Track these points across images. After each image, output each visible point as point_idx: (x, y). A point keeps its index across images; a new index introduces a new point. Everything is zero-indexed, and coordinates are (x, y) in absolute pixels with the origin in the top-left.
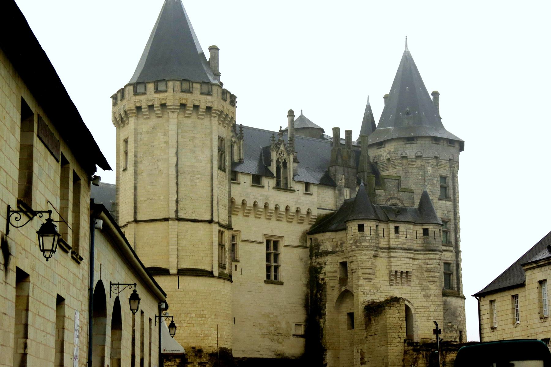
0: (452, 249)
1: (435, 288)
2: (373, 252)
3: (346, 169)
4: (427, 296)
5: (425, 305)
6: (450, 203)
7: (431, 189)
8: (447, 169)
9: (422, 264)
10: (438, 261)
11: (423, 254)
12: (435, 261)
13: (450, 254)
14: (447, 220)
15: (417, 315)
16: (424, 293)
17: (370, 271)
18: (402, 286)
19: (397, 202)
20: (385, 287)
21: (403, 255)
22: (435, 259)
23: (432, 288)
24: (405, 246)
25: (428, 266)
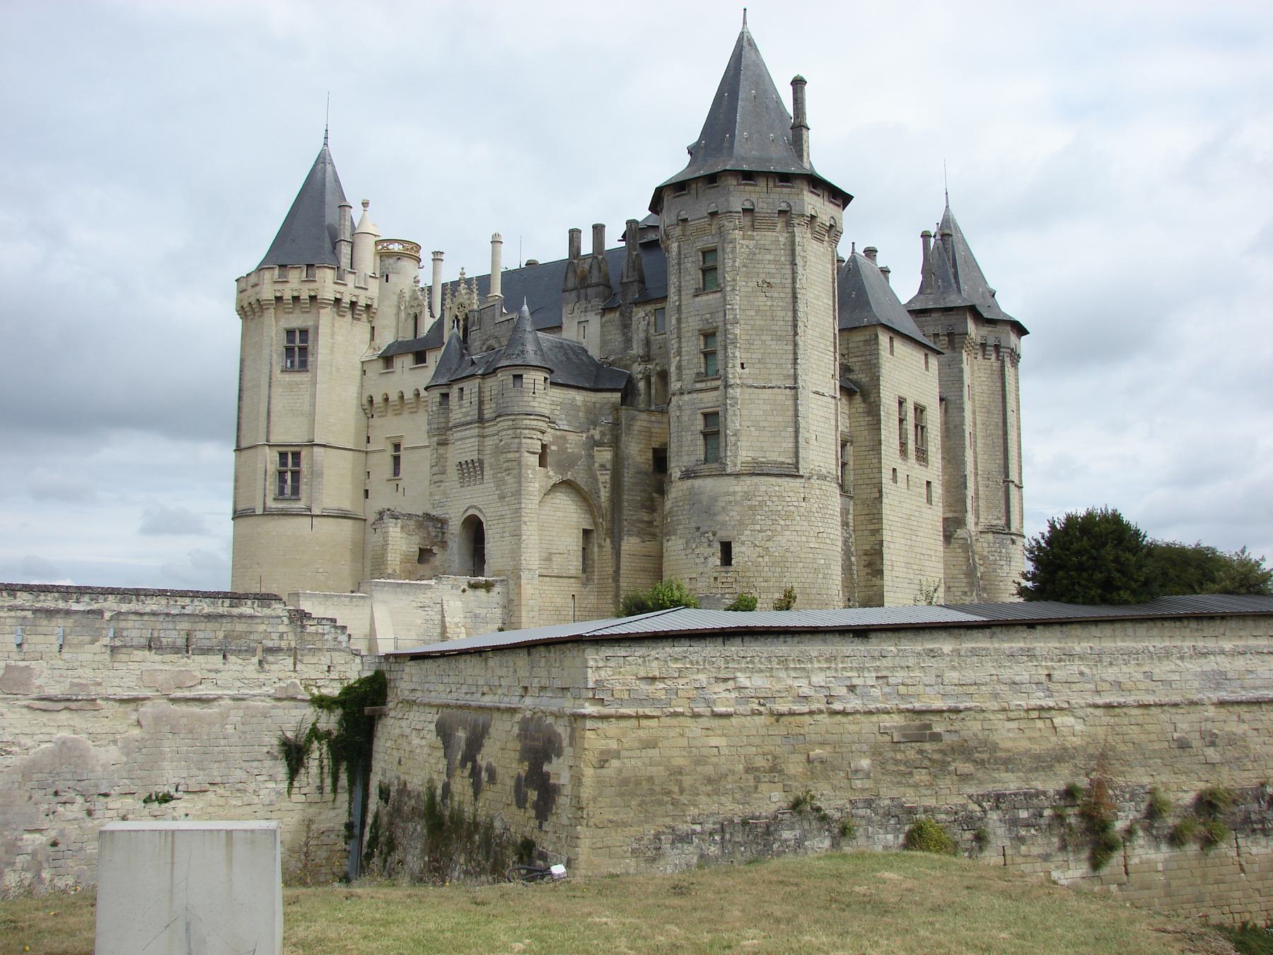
0: (718, 383)
1: (512, 481)
2: (435, 439)
3: (582, 292)
4: (502, 497)
5: (499, 514)
6: (719, 295)
7: (674, 283)
8: (714, 232)
9: (498, 441)
10: (510, 432)
11: (496, 425)
12: (504, 433)
13: (715, 393)
14: (711, 331)
15: (490, 532)
16: (498, 492)
17: (436, 468)
18: (475, 485)
19: (492, 342)
20: (454, 491)
21: (467, 432)
22: (504, 430)
23: (509, 482)
24: (468, 418)
25: (502, 443)
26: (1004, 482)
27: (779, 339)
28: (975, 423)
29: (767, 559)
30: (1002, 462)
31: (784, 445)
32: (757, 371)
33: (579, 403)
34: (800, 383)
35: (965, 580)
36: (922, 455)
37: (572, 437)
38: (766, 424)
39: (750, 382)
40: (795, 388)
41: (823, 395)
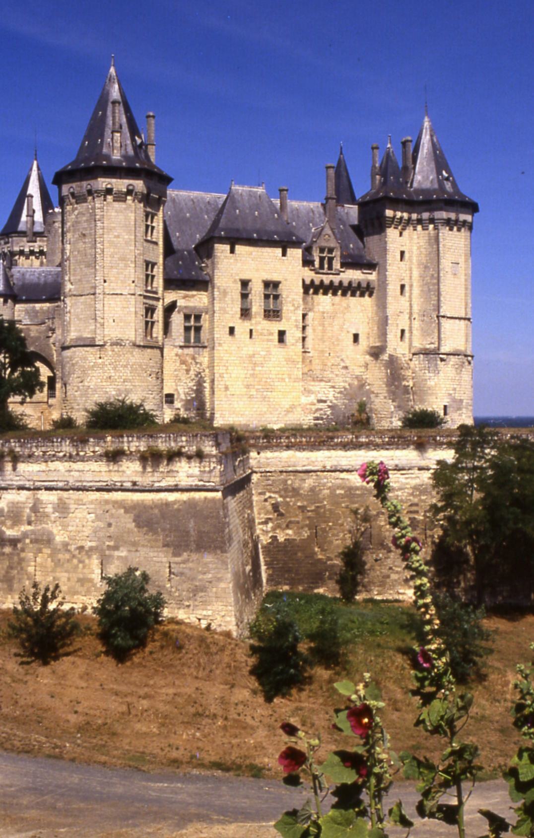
26: (438, 317)
27: (88, 266)
28: (411, 277)
29: (79, 393)
30: (435, 302)
31: (91, 328)
32: (77, 286)
33: (38, 309)
34: (98, 291)
35: (386, 389)
36: (273, 314)
37: (32, 328)
38: (82, 316)
39: (75, 293)
40: (94, 294)
41: (121, 294)
